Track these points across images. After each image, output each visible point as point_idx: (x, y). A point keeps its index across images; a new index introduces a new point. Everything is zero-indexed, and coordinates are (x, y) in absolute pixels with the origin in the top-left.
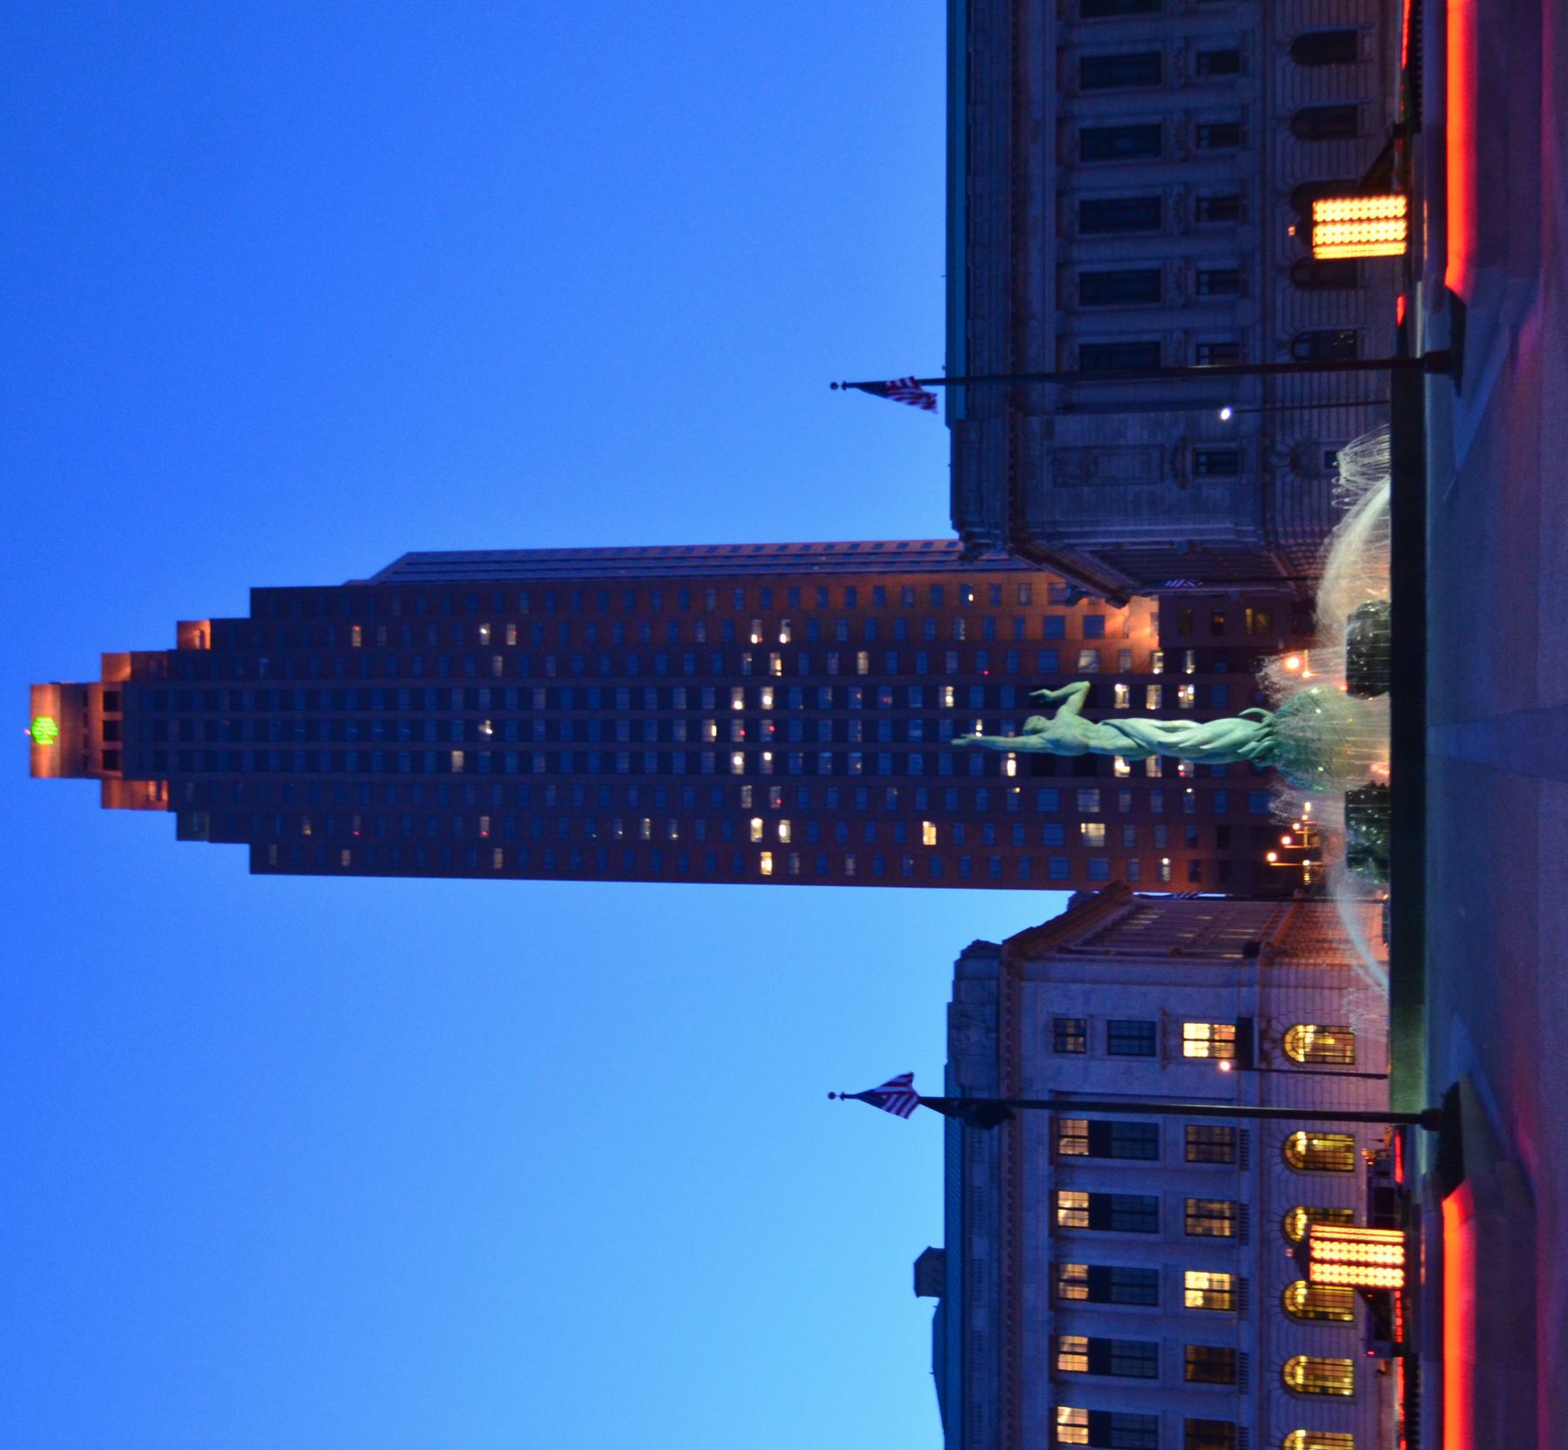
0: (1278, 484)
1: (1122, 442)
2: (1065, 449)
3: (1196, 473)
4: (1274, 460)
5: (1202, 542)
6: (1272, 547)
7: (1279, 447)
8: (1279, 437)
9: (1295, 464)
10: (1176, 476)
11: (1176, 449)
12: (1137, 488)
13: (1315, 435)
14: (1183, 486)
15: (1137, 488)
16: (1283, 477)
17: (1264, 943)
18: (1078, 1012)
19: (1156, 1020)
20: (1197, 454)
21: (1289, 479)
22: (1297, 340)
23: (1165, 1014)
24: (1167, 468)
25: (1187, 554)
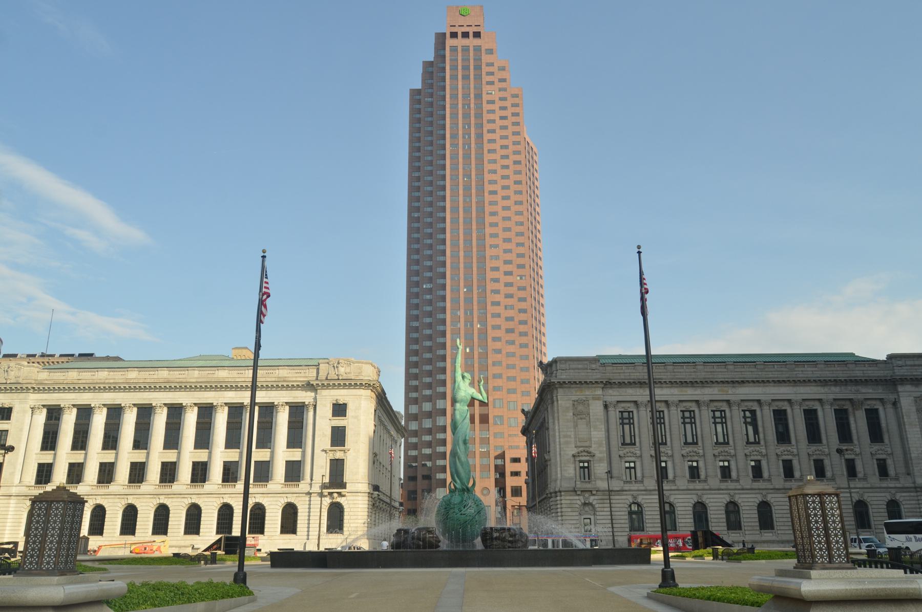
0: (577, 497)
1: (592, 429)
2: (589, 405)
3: (581, 462)
4: (587, 495)
5: (550, 465)
6: (549, 495)
7: (592, 498)
8: (596, 497)
9: (585, 504)
10: (579, 453)
11: (590, 453)
12: (572, 436)
13: (598, 513)
14: (574, 456)
15: (572, 436)
16: (579, 500)
17: (380, 494)
18: (350, 412)
19: (346, 447)
20: (588, 462)
21: (578, 502)
22: (639, 505)
23: (348, 450)
24: (581, 449)
25: (545, 458)
